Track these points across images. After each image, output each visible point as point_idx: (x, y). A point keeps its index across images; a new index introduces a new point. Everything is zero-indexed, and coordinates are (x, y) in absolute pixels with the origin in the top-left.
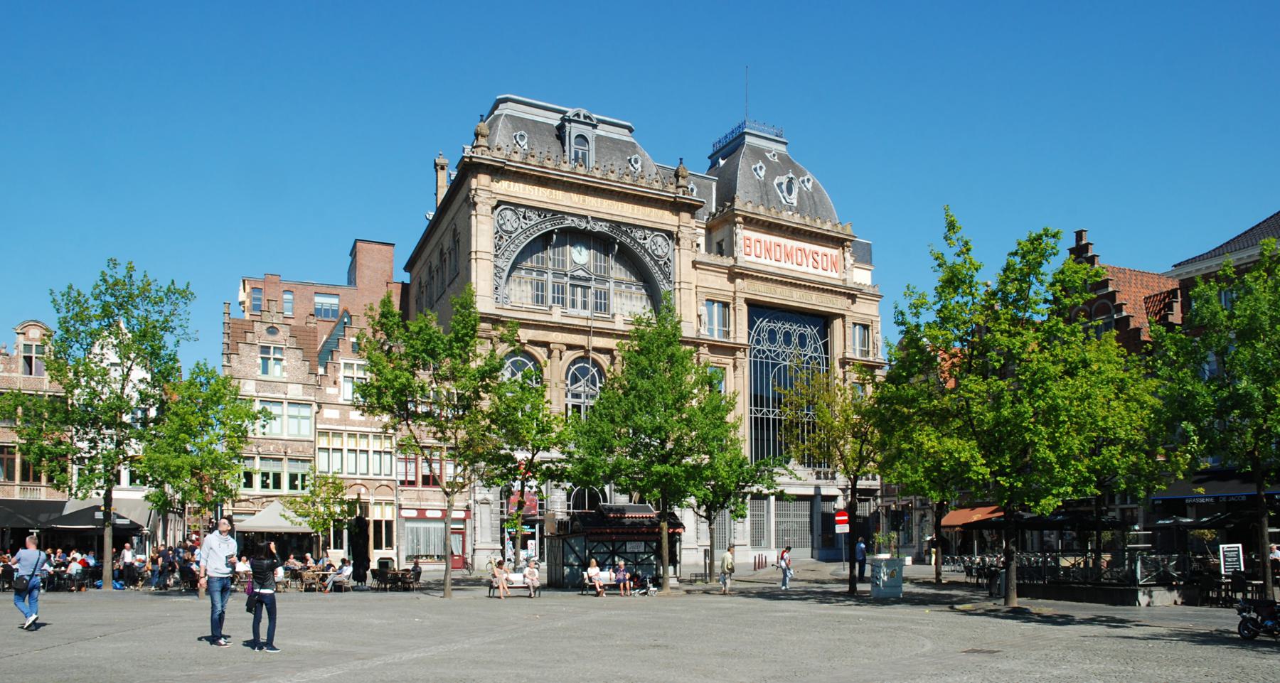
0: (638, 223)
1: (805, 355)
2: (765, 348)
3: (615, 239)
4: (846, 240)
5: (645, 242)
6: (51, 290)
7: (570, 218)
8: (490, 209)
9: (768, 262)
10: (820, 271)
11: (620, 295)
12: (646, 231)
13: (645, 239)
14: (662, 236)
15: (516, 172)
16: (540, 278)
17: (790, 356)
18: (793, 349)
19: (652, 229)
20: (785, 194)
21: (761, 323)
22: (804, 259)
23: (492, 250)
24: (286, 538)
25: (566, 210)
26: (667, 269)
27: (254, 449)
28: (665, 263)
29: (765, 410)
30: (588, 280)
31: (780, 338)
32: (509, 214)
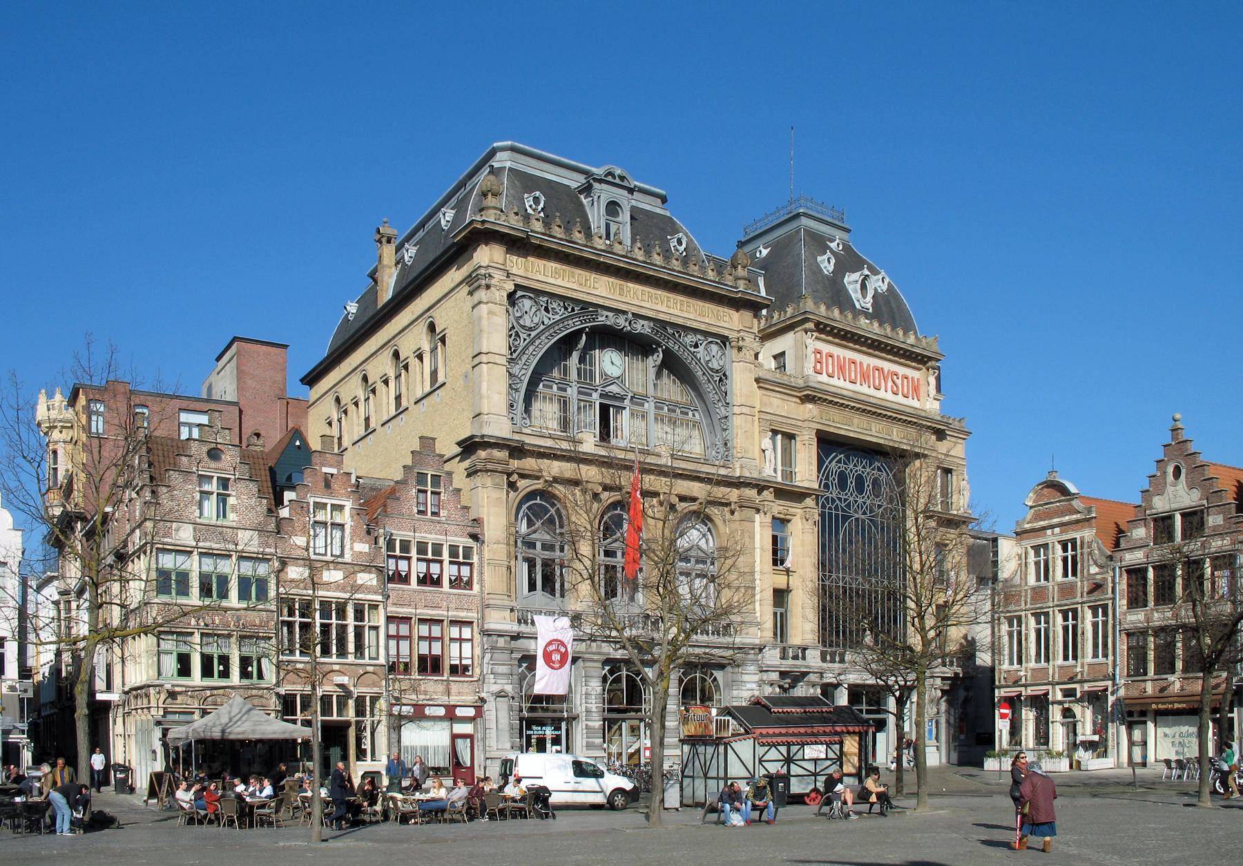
0: (689, 324)
1: (880, 506)
2: (834, 495)
3: (659, 345)
4: (930, 359)
5: (695, 350)
6: (469, 475)
7: (606, 313)
8: (505, 295)
9: (841, 383)
10: (899, 399)
11: (662, 420)
12: (699, 336)
13: (696, 346)
14: (717, 343)
15: (540, 246)
16: (563, 394)
17: (861, 505)
18: (866, 499)
19: (706, 334)
20: (860, 296)
21: (830, 463)
22: (883, 381)
23: (505, 351)
24: (238, 744)
25: (601, 302)
26: (723, 388)
27: (193, 622)
28: (721, 380)
29: (834, 576)
30: (622, 399)
31: (851, 483)
32: (527, 303)
